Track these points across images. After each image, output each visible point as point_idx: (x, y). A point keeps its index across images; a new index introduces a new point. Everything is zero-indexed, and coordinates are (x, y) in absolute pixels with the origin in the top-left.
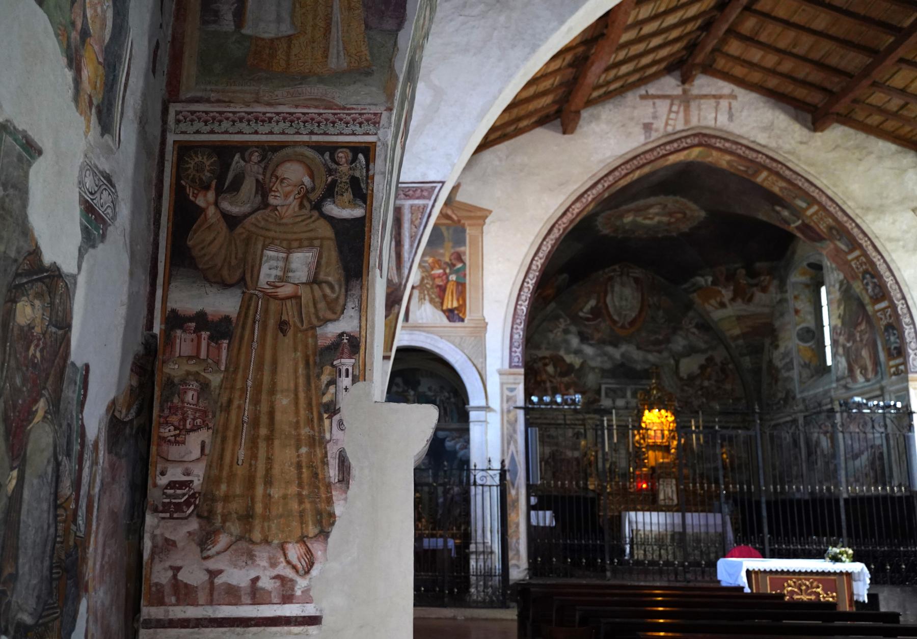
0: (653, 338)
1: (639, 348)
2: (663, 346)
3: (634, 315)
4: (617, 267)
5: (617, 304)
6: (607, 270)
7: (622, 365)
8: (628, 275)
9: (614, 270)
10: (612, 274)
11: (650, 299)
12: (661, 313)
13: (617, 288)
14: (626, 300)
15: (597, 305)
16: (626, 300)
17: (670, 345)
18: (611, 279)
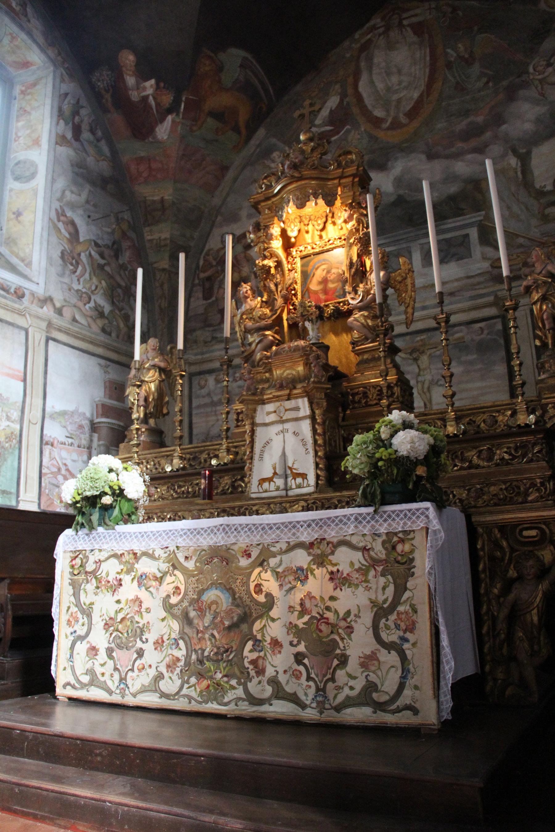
0: (462, 125)
1: (431, 156)
2: (488, 135)
3: (416, 95)
4: (376, 21)
5: (380, 86)
6: (357, 36)
7: (400, 201)
8: (401, 25)
9: (374, 28)
10: (369, 36)
11: (449, 50)
12: (476, 69)
13: (379, 58)
14: (399, 72)
15: (341, 100)
16: (399, 72)
17: (504, 127)
18: (366, 47)
